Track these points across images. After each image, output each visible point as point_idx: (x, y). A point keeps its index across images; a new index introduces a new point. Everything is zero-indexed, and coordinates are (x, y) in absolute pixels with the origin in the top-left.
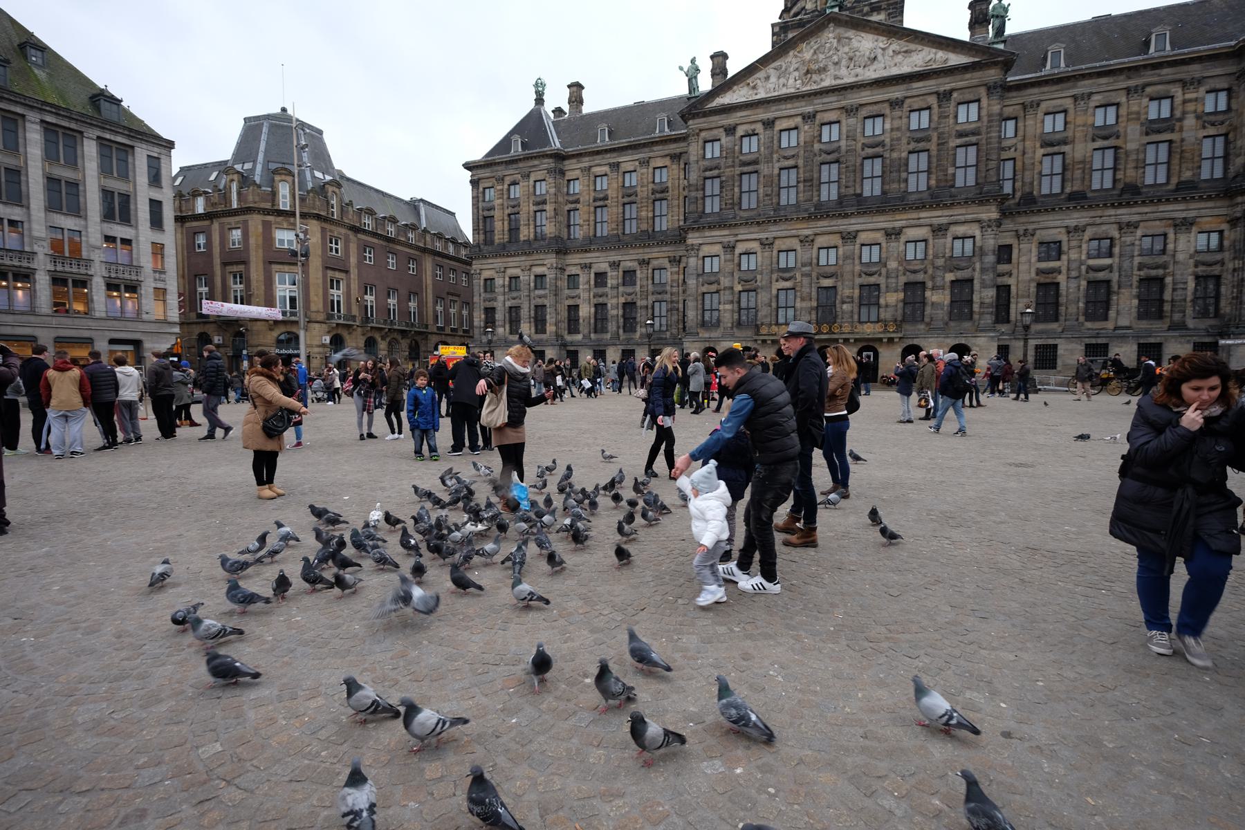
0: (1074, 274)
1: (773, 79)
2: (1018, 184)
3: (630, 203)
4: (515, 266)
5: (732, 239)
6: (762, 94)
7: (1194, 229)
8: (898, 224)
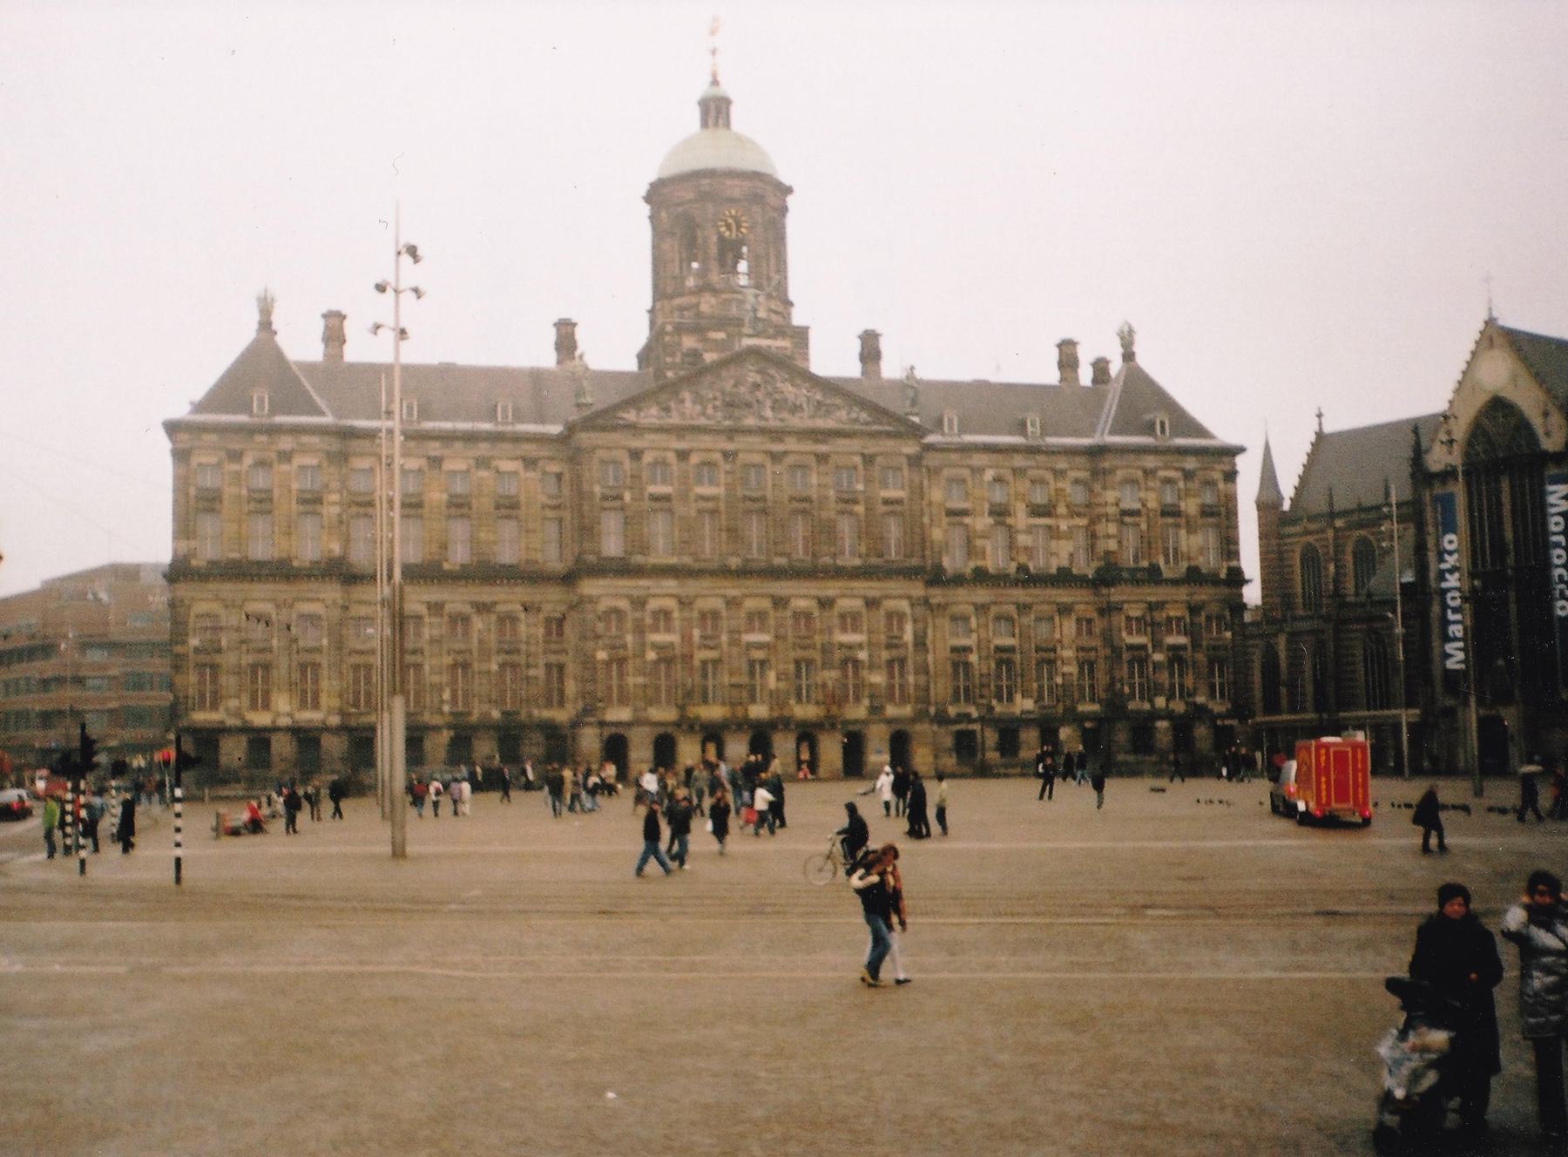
0: (984, 654)
1: (688, 404)
2: (928, 553)
3: (462, 516)
4: (261, 597)
5: (642, 593)
6: (675, 420)
7: (1074, 617)
8: (830, 593)
